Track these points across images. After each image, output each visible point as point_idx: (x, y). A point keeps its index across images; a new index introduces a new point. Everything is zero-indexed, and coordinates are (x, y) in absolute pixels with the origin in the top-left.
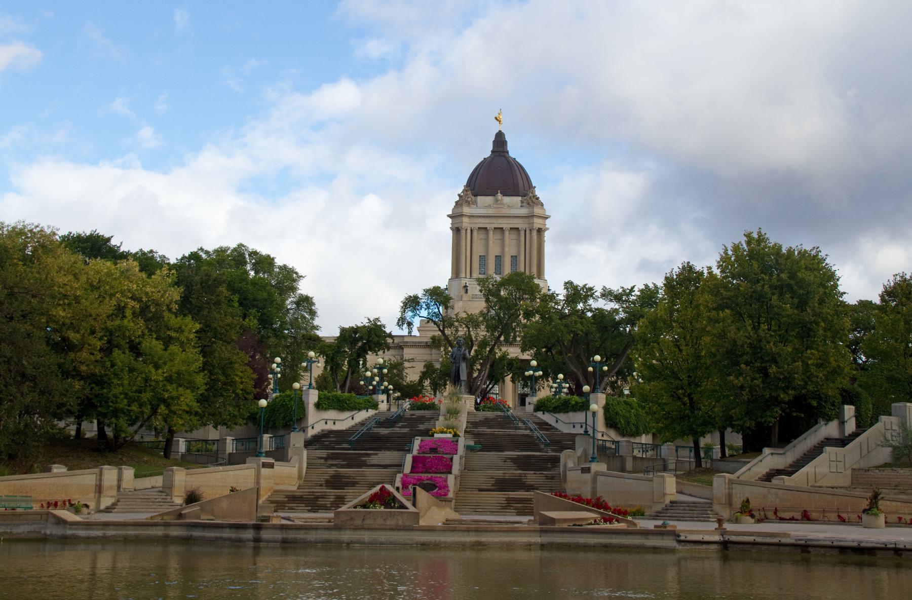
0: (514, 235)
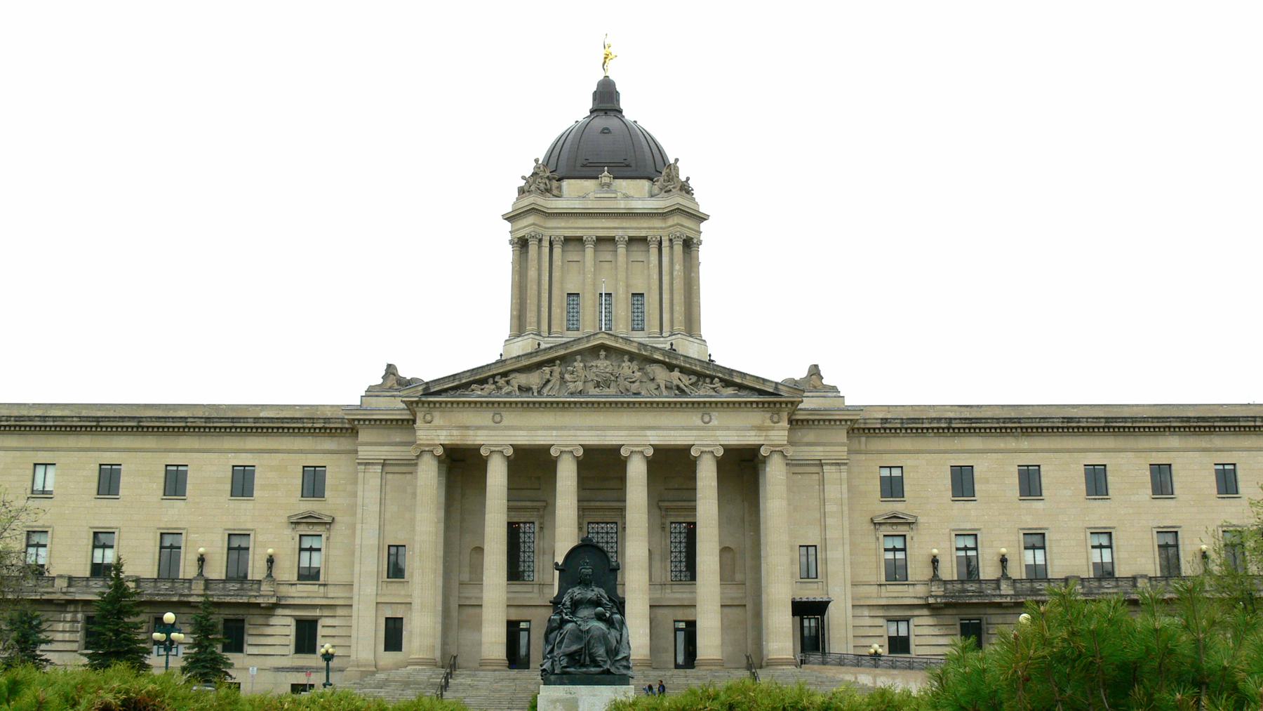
0: (637, 251)
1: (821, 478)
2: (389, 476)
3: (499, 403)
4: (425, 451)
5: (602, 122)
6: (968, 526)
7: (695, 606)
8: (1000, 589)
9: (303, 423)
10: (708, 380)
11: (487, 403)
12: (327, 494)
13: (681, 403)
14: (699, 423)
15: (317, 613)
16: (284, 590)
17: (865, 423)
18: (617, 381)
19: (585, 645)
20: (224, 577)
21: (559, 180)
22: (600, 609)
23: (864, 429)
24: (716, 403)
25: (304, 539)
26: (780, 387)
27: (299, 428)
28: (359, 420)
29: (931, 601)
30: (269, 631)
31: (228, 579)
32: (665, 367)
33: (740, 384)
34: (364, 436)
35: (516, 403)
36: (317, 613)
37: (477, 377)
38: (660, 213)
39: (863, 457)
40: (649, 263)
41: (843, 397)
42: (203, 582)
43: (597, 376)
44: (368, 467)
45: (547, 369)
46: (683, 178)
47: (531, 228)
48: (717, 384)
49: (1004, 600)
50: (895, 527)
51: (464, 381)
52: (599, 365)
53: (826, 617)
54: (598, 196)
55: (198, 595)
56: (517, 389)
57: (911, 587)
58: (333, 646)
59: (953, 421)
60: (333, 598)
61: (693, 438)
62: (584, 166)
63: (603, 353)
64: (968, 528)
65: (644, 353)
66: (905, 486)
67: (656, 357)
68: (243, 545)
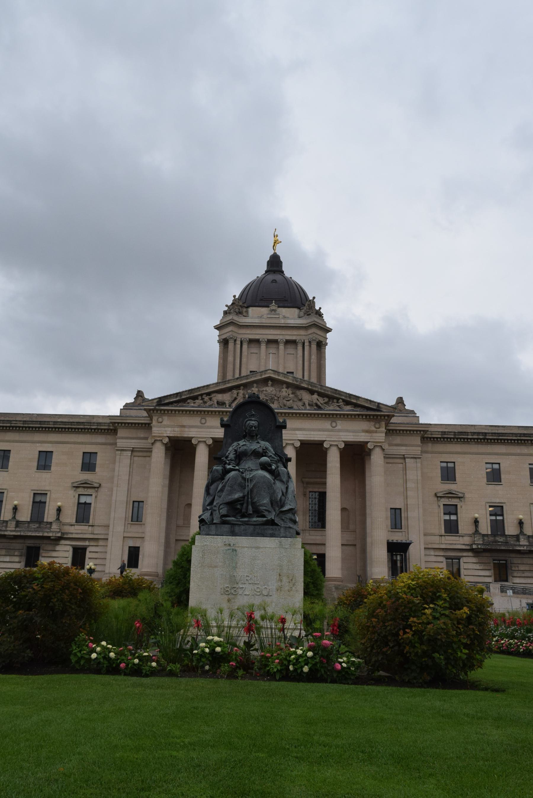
0: (291, 350)
1: (404, 466)
2: (136, 458)
3: (204, 411)
4: (157, 440)
5: (271, 277)
6: (498, 501)
7: (325, 544)
8: (519, 542)
9: (84, 425)
10: (335, 401)
11: (197, 411)
12: (97, 469)
13: (318, 414)
14: (329, 427)
15: (87, 543)
16: (67, 529)
17: (431, 434)
18: (278, 400)
19: (248, 493)
20: (29, 520)
21: (248, 307)
22: (264, 459)
23: (430, 438)
24: (340, 415)
25: (81, 497)
26: (381, 406)
27: (82, 429)
28: (118, 423)
29: (474, 547)
30: (54, 554)
31: (32, 521)
32: (308, 392)
33: (356, 403)
34: (121, 433)
35: (215, 412)
36: (87, 543)
37: (192, 395)
38: (304, 327)
39: (430, 455)
40: (297, 355)
41: (419, 417)
42: (15, 523)
43: (266, 396)
44: (122, 452)
45: (235, 392)
46: (317, 308)
47: (230, 333)
48: (341, 403)
49: (522, 548)
50: (450, 500)
51: (183, 397)
52: (267, 390)
53: (407, 553)
54: (269, 316)
55: (11, 531)
56: (216, 403)
57: (461, 538)
58: (95, 565)
59: (487, 435)
60: (97, 534)
61: (325, 436)
62: (261, 300)
63: (270, 383)
64: (497, 502)
65: (295, 383)
66: (456, 474)
67: (303, 385)
68: (43, 500)
